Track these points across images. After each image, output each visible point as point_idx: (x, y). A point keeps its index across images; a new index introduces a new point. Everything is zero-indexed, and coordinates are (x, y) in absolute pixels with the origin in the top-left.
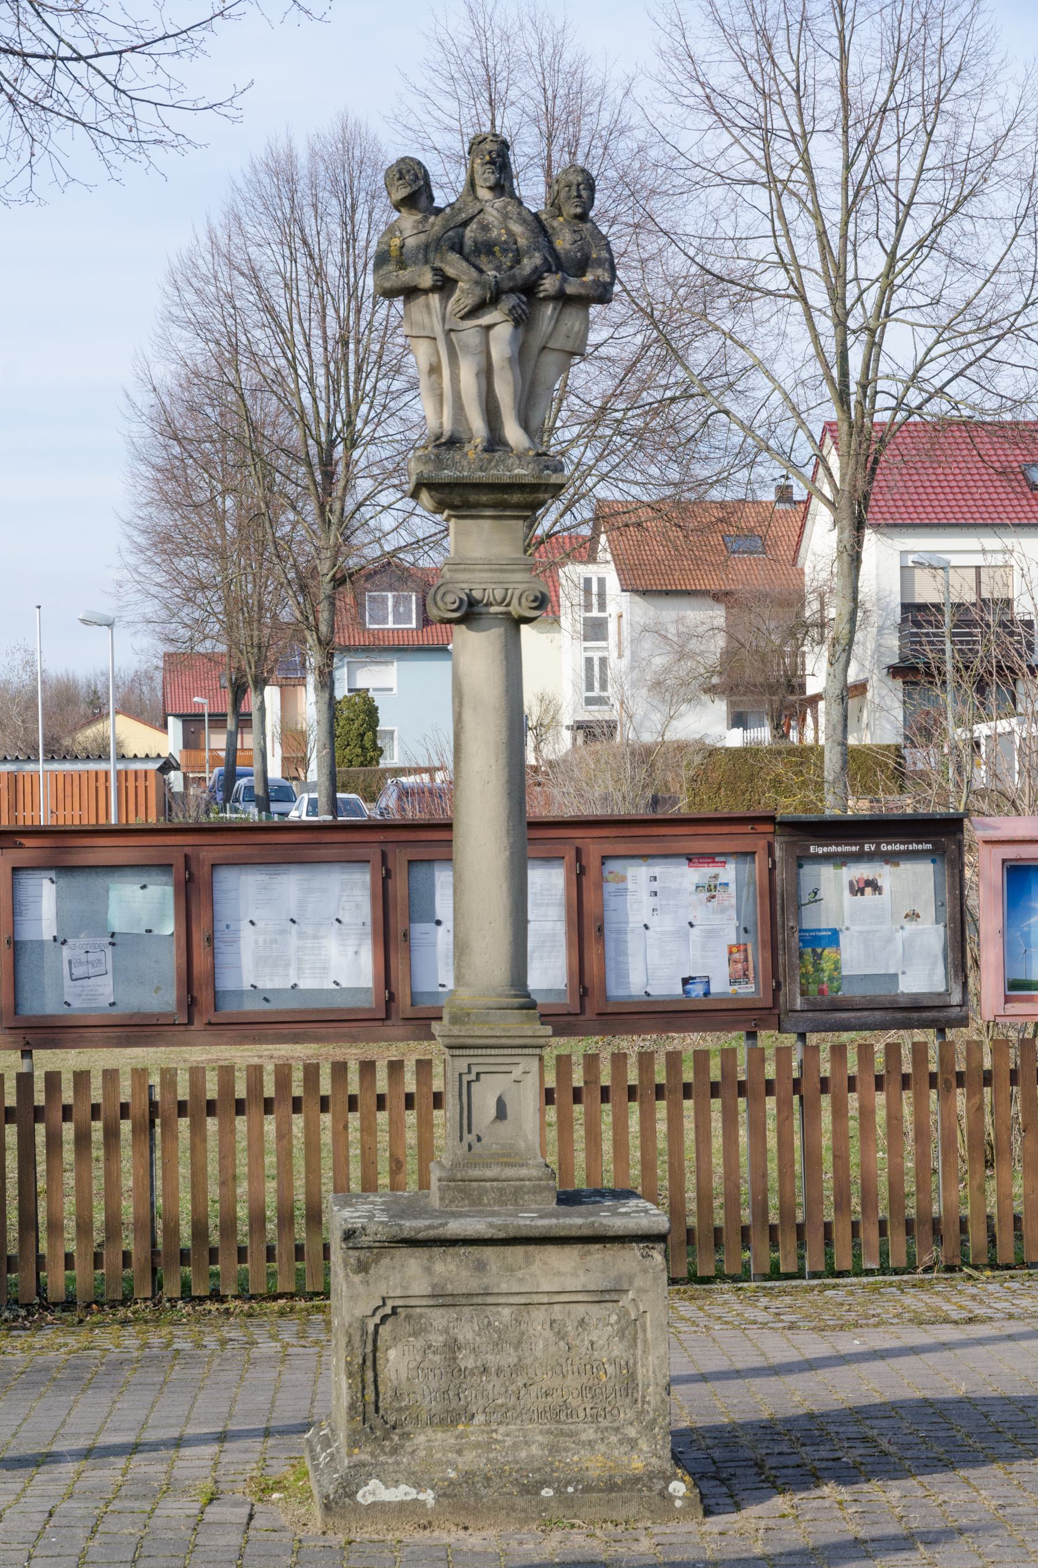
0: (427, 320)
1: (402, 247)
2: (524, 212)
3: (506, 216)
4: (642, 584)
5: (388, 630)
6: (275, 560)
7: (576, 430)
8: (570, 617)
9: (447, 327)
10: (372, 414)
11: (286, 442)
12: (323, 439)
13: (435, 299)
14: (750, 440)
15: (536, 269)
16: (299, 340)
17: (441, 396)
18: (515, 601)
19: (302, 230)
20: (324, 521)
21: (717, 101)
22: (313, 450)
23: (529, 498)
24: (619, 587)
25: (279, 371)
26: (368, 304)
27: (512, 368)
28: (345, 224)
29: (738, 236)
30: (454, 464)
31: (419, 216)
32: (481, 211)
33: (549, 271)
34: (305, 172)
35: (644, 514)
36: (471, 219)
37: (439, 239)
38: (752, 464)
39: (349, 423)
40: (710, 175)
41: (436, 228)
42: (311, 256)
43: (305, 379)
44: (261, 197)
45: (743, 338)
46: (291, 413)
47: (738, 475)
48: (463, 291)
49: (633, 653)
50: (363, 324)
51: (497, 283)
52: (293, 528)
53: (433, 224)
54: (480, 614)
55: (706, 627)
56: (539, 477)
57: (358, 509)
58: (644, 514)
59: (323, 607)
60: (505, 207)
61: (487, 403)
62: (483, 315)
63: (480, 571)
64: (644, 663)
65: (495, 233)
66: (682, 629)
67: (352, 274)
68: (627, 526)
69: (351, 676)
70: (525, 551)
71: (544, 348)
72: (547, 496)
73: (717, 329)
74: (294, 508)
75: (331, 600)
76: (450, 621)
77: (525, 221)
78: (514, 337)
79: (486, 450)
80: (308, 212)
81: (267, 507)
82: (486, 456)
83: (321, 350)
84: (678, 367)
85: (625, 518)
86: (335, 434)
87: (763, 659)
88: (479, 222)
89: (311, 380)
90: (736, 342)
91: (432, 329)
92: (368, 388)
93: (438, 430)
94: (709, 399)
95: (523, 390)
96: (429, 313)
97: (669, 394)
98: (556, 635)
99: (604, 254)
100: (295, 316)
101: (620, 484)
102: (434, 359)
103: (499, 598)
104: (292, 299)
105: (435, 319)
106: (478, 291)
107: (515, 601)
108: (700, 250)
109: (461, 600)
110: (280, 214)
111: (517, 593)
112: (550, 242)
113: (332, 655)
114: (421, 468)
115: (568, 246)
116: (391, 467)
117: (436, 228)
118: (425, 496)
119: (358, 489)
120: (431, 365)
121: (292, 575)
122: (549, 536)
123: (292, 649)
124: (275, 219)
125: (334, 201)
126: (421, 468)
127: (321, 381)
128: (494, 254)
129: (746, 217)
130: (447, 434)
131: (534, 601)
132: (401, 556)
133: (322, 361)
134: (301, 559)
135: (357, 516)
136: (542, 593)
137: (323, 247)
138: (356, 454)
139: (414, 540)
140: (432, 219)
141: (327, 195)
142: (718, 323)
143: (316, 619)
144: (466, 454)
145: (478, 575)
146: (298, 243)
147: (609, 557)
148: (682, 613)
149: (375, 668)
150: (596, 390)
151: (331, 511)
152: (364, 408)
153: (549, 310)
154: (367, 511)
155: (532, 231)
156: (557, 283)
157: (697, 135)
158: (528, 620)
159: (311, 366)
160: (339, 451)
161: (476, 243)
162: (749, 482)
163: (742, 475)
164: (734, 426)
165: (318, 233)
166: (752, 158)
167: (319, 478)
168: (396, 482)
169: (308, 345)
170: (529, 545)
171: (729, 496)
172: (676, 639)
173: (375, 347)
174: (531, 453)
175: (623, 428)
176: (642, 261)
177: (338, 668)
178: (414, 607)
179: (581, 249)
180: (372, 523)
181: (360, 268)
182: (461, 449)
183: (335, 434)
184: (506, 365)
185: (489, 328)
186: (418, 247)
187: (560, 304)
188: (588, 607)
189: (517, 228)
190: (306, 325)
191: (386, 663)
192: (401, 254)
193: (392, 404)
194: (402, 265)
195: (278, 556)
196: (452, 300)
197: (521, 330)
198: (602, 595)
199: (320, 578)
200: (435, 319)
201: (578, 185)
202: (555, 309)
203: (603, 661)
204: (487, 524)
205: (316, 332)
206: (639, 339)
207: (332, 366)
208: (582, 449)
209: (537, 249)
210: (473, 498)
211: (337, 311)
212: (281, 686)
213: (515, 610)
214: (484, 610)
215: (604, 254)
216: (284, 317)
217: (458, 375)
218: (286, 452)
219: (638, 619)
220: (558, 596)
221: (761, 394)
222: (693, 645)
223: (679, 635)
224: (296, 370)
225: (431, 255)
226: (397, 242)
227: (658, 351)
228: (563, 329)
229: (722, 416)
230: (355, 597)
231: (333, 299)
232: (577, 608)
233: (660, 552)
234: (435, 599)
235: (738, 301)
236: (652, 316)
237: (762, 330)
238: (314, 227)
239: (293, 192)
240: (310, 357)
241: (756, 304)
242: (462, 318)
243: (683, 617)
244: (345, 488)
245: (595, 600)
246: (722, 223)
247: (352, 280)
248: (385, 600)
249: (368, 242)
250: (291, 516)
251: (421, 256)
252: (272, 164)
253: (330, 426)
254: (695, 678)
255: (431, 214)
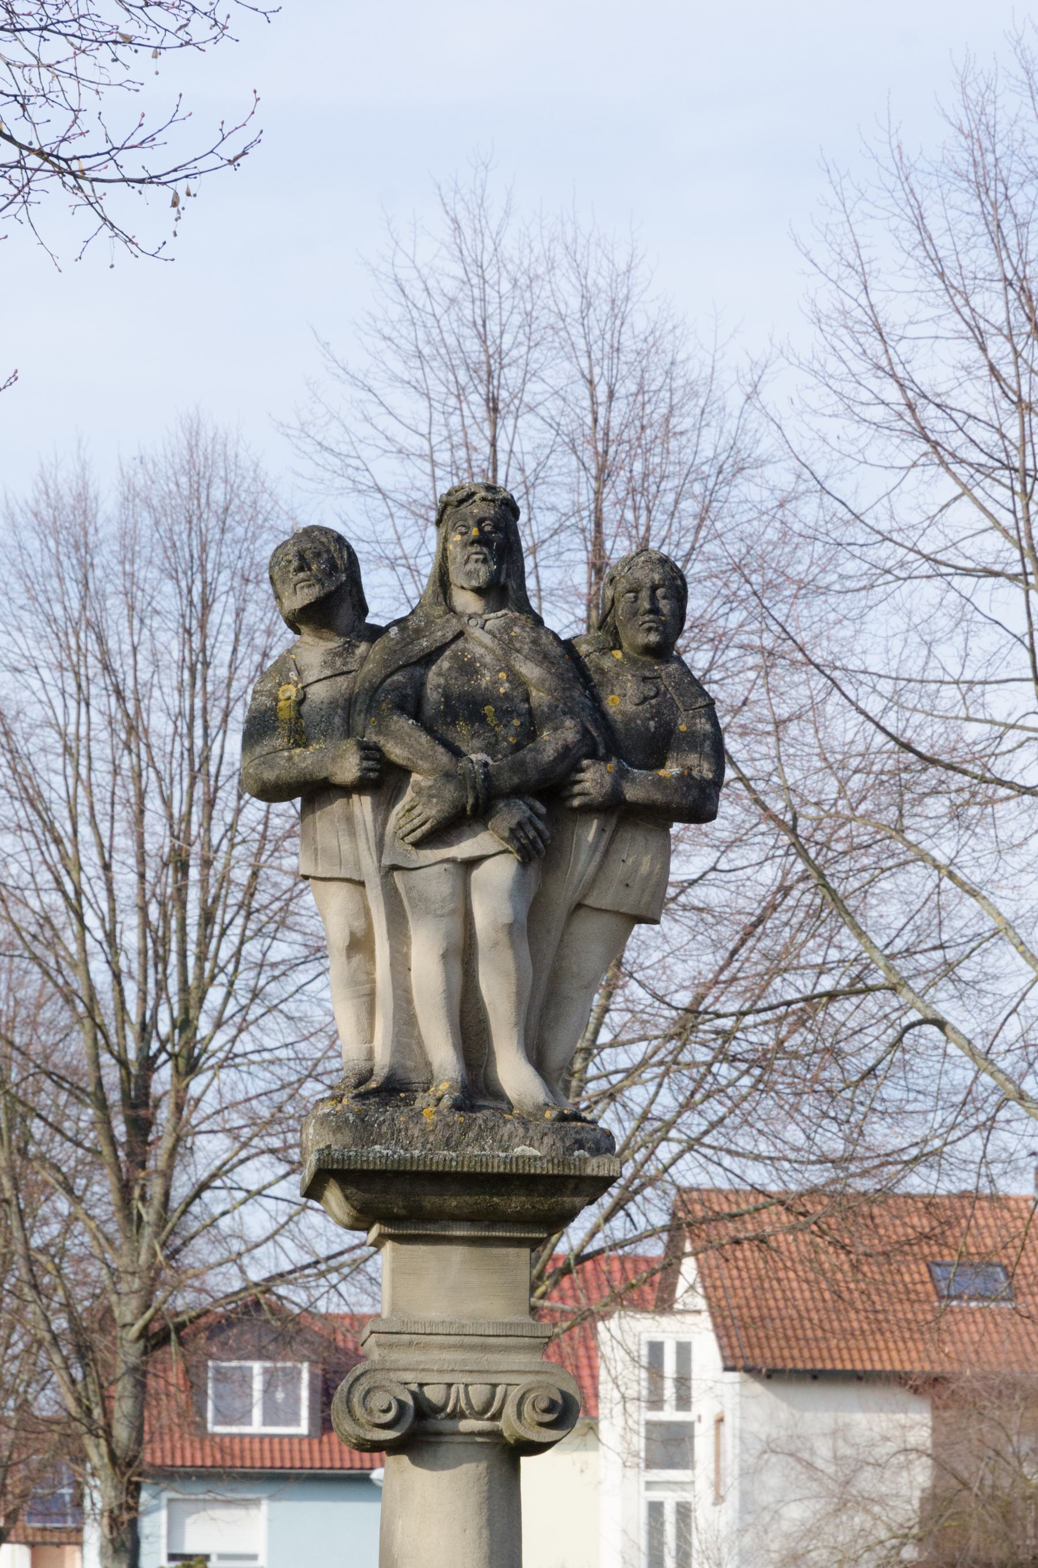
0: (346, 847)
1: (301, 702)
2: (544, 640)
3: (508, 646)
4: (765, 1359)
5: (252, 1437)
6: (28, 1293)
7: (639, 1050)
8: (619, 1421)
9: (386, 861)
10: (231, 1008)
11: (56, 1058)
12: (132, 1055)
13: (363, 806)
14: (985, 1078)
15: (566, 750)
16: (91, 866)
17: (371, 995)
18: (510, 1410)
19: (101, 640)
20: (128, 1218)
21: (929, 414)
22: (112, 1075)
23: (544, 1204)
24: (719, 1364)
25: (47, 919)
26: (227, 797)
27: (513, 945)
28: (188, 632)
29: (968, 676)
30: (395, 1132)
31: (335, 643)
32: (460, 635)
33: (592, 755)
34: (113, 528)
35: (773, 1219)
36: (440, 650)
37: (375, 689)
38: (989, 1126)
39: (185, 1024)
40: (912, 556)
41: (369, 666)
42: (119, 694)
43: (100, 935)
44: (23, 576)
45: (975, 876)
46: (68, 1000)
47: (964, 1146)
48: (419, 792)
49: (745, 1496)
50: (217, 832)
51: (487, 776)
52: (67, 1230)
53: (364, 659)
54: (439, 1434)
55: (891, 1447)
56: (562, 1163)
57: (197, 1195)
58: (773, 1219)
59: (123, 1390)
60: (507, 628)
61: (463, 1014)
62: (459, 839)
63: (442, 1347)
64: (767, 1517)
65: (486, 680)
66: (845, 1450)
67: (198, 731)
68: (737, 1242)
69: (174, 1528)
70: (533, 1288)
71: (579, 906)
72: (577, 1200)
73: (923, 857)
74: (69, 1190)
75: (140, 1376)
76: (376, 1447)
77: (546, 656)
78: (520, 884)
79: (458, 1106)
80: (116, 606)
81: (16, 1187)
82: (458, 1117)
83: (133, 878)
84: (845, 930)
85: (731, 1228)
86: (155, 1046)
87: (1007, 1514)
88: (455, 657)
89: (111, 937)
90: (961, 884)
91: (357, 864)
92: (225, 953)
93: (364, 1065)
94: (905, 997)
95: (532, 997)
96: (352, 833)
97: (827, 983)
98: (589, 1456)
99: (703, 725)
100: (83, 809)
101: (727, 1161)
102: (359, 925)
103: (477, 1402)
104: (78, 777)
105: (362, 845)
106: (450, 792)
107: (510, 1410)
108: (895, 701)
109: (401, 1405)
110: (58, 611)
111: (515, 1393)
112: (596, 700)
113: (138, 1487)
114: (327, 1139)
115: (630, 708)
116: (265, 1113)
117: (369, 666)
118: (333, 1194)
119: (199, 1156)
120: (352, 934)
121: (60, 1323)
122: (581, 1259)
123: (57, 1472)
124: (51, 620)
125: (169, 587)
126: (327, 1139)
127: (130, 939)
128: (483, 719)
129: (987, 640)
130: (381, 1072)
131: (547, 1411)
132: (282, 1290)
133: (135, 900)
134: (80, 1292)
135: (196, 1208)
136: (564, 1395)
137: (144, 676)
138: (196, 1085)
139: (308, 1259)
140: (363, 648)
141: (153, 574)
142: (926, 845)
143: (106, 1412)
144: (419, 1114)
145: (436, 1355)
146: (94, 666)
147: (701, 1303)
148: (844, 1417)
149: (221, 1513)
150: (682, 971)
151: (143, 1198)
152: (215, 996)
153: (590, 832)
154: (214, 1201)
155: (561, 677)
156: (608, 779)
157: (892, 478)
158: (537, 1448)
159: (113, 910)
160: (163, 1079)
161: (447, 696)
162: (985, 1161)
163: (970, 1146)
164: (952, 1049)
165: (135, 649)
166: (997, 524)
167: (120, 1129)
168: (276, 1143)
169: (107, 867)
170: (540, 1277)
171: (946, 1187)
172: (831, 1470)
173: (241, 875)
174: (549, 1114)
175: (734, 1047)
176: (780, 724)
177: (148, 1512)
178: (305, 1394)
179: (657, 714)
180: (225, 1223)
181: (215, 718)
182: (408, 1102)
183: (155, 1046)
184: (503, 937)
185: (471, 864)
186: (333, 704)
187: (614, 821)
188: (656, 1402)
189: (530, 671)
190: (104, 827)
191: (245, 1503)
192: (299, 715)
193: (272, 988)
194: (300, 737)
195: (35, 1287)
196: (399, 808)
197: (533, 871)
198: (683, 1381)
199: (118, 1332)
200: (362, 845)
201: (654, 588)
202: (601, 830)
203: (684, 1512)
204: (456, 1254)
205: (124, 843)
206: (769, 874)
207: (154, 911)
208: (652, 1088)
209: (570, 712)
210: (430, 1202)
211: (167, 802)
212: (32, 1545)
213: (510, 1426)
214: (447, 1425)
215: (703, 725)
216: (60, 812)
217: (406, 957)
218: (59, 1081)
219: (755, 1427)
220: (594, 1377)
221: (1010, 988)
222: (867, 1482)
223: (837, 1459)
224: (80, 917)
225: (359, 720)
226: (290, 691)
227: (807, 899)
228: (618, 870)
229: (932, 1030)
230: (187, 1371)
231: (160, 779)
232: (631, 1407)
233: (802, 1294)
234: (348, 1401)
235: (967, 803)
236: (793, 830)
237: (1015, 861)
238: (127, 639)
239: (86, 567)
240: (110, 890)
241: (1001, 809)
242: (418, 844)
243: (847, 1426)
244: (173, 1153)
245: (669, 1391)
246: (938, 650)
247: (199, 743)
248: (246, 1379)
249: (233, 667)
250: (63, 1205)
251: (337, 721)
252: (46, 514)
253: (146, 1030)
254: (869, 1549)
255: (361, 638)
